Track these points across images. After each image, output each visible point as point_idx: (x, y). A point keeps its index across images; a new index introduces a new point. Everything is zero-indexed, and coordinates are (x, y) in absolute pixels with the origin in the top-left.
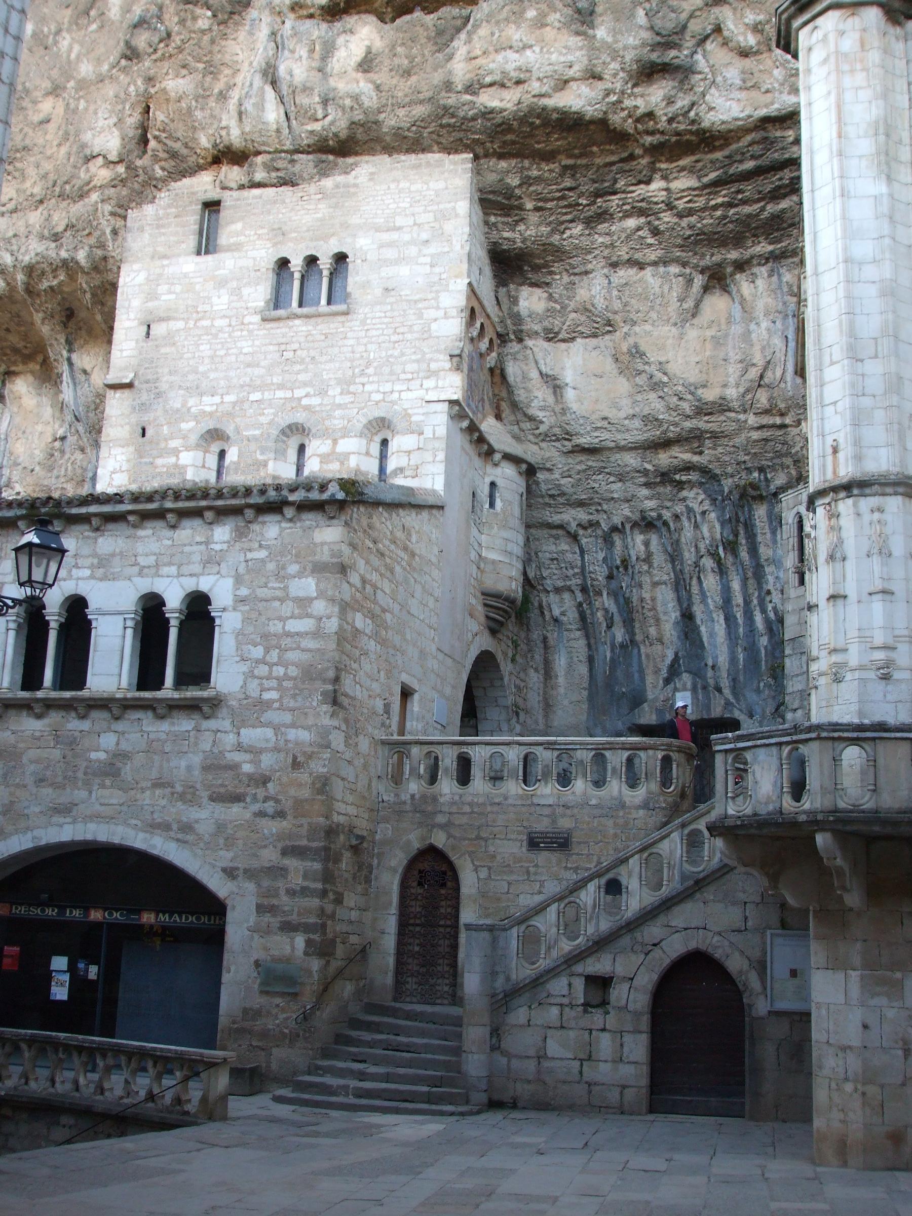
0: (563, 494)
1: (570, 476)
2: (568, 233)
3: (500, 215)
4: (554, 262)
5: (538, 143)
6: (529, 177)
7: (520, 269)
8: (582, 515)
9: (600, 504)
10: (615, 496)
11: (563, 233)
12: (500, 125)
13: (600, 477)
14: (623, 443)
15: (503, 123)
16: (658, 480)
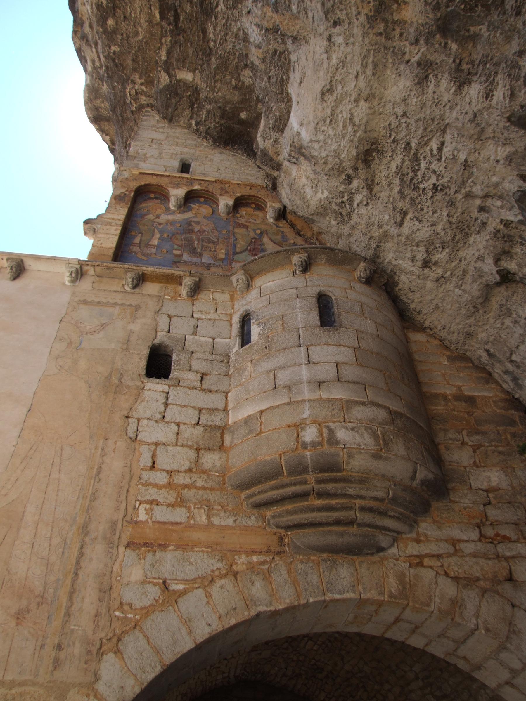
0: (430, 246)
1: (405, 214)
2: (212, 44)
3: (193, 113)
4: (238, 78)
5: (137, 34)
6: (166, 62)
7: (242, 122)
8: (480, 243)
9: (469, 196)
10: (462, 157)
11: (211, 49)
12: (116, 66)
13: (423, 165)
14: (362, 84)
15: (113, 60)
16: (454, 46)
